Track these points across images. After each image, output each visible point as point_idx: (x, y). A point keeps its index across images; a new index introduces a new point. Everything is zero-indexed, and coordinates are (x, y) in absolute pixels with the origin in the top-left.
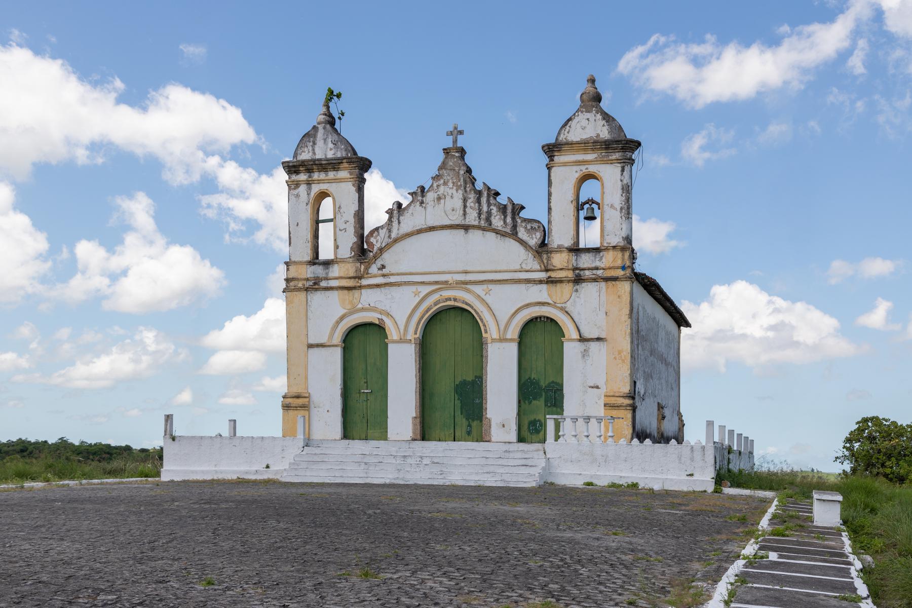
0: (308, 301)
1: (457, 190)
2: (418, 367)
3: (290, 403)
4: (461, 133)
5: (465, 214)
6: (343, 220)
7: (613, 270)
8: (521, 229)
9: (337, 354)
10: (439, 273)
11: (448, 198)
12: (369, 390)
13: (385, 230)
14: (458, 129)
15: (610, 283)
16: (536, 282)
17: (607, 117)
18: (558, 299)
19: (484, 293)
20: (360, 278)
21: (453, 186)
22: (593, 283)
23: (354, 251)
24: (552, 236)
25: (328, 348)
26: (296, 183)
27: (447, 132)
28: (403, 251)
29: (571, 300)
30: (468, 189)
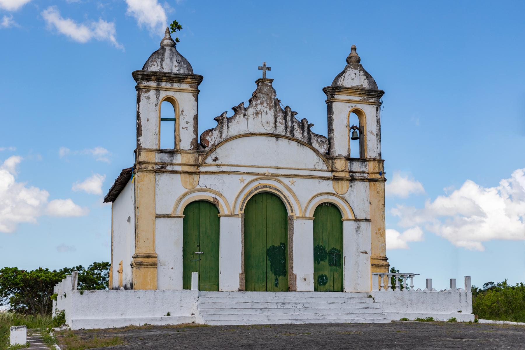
0: (157, 181)
1: (270, 109)
2: (243, 235)
3: (141, 262)
4: (269, 69)
5: (276, 127)
6: (185, 121)
7: (374, 174)
8: (314, 141)
9: (180, 222)
10: (259, 167)
11: (264, 114)
12: (202, 252)
13: (217, 132)
14: (267, 66)
15: (372, 183)
16: (325, 179)
17: (367, 74)
18: (340, 191)
19: (291, 184)
20: (199, 166)
21: (267, 105)
22: (362, 182)
23: (193, 145)
24: (334, 148)
25: (173, 218)
27: (259, 67)
28: (232, 148)
29: (348, 193)
30: (278, 110)
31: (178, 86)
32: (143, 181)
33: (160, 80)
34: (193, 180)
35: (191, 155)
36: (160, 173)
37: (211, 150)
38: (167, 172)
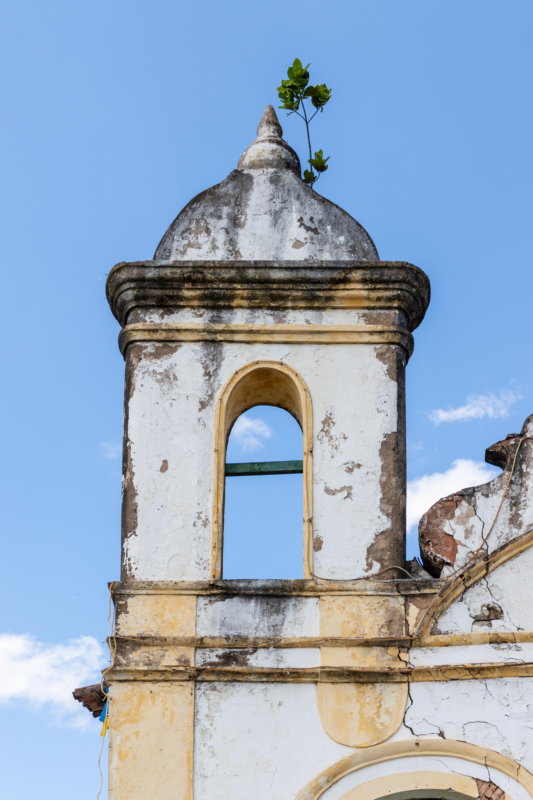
6: (341, 459)
23: (380, 560)
26: (162, 336)
31: (307, 321)
32: (137, 721)
33: (222, 303)
34: (380, 707)
35: (368, 600)
36: (216, 684)
37: (466, 575)
38: (252, 678)
